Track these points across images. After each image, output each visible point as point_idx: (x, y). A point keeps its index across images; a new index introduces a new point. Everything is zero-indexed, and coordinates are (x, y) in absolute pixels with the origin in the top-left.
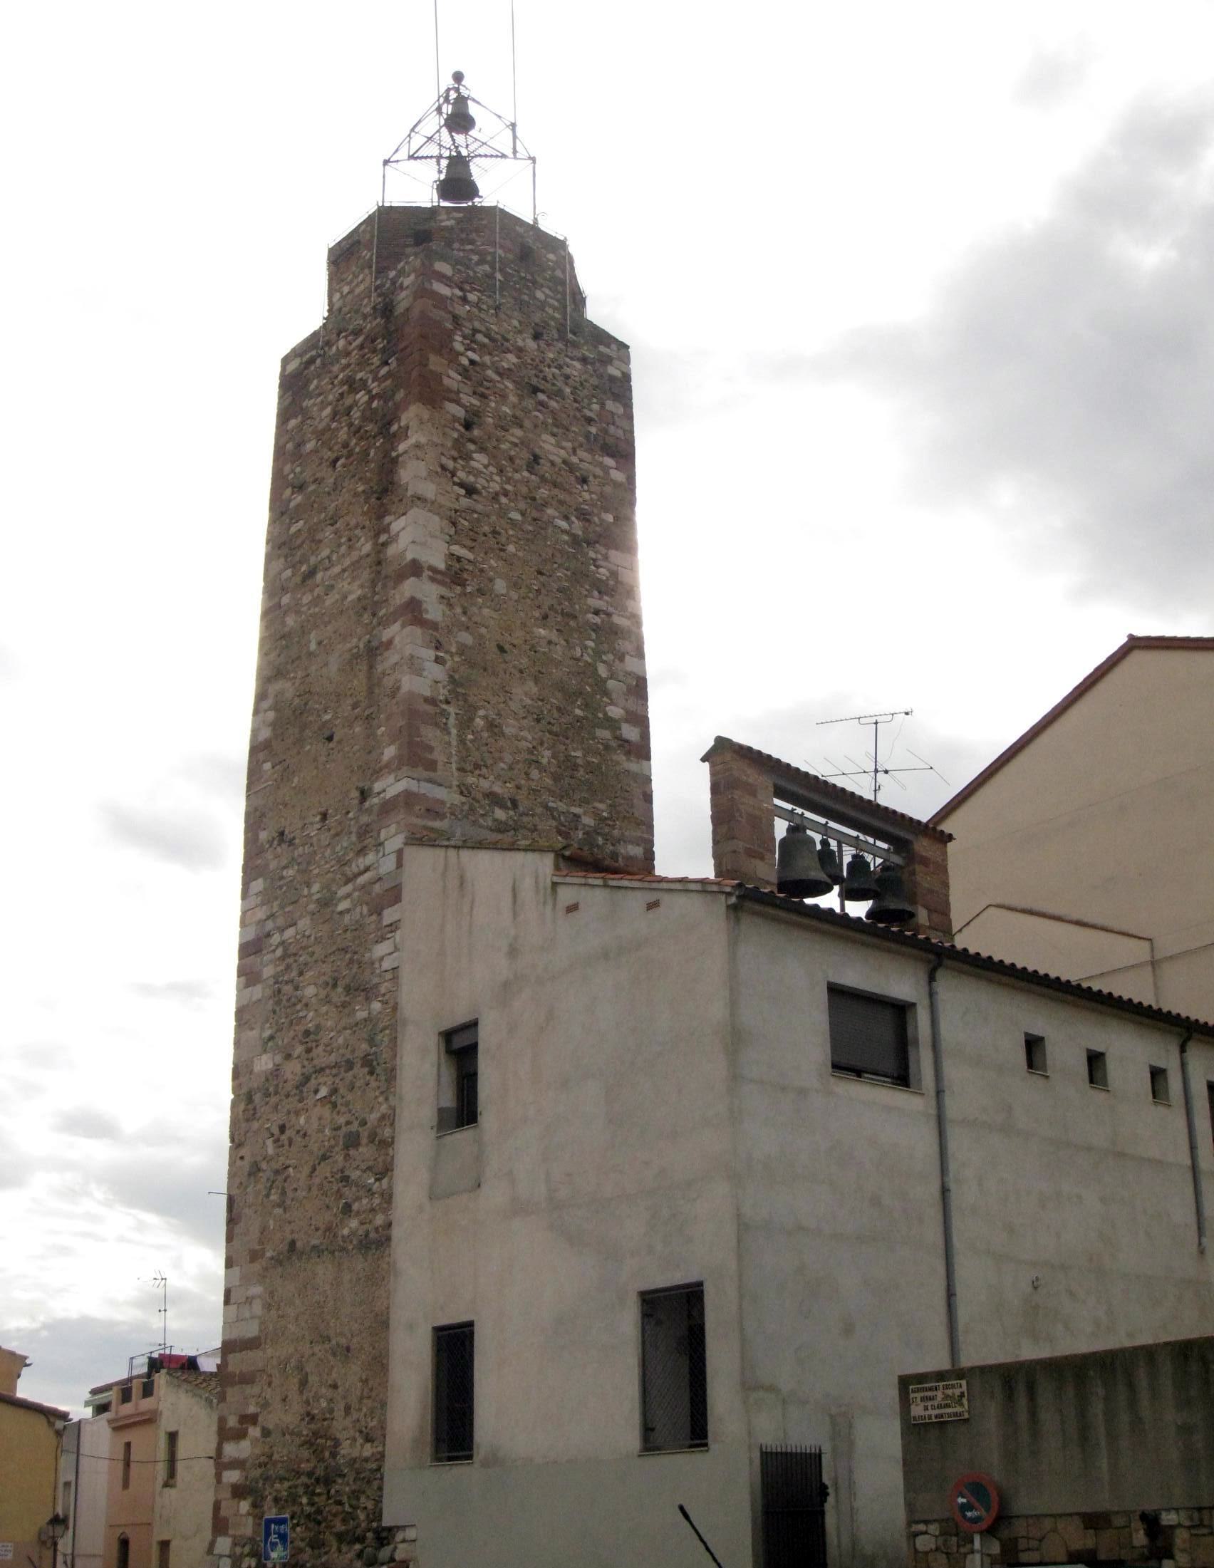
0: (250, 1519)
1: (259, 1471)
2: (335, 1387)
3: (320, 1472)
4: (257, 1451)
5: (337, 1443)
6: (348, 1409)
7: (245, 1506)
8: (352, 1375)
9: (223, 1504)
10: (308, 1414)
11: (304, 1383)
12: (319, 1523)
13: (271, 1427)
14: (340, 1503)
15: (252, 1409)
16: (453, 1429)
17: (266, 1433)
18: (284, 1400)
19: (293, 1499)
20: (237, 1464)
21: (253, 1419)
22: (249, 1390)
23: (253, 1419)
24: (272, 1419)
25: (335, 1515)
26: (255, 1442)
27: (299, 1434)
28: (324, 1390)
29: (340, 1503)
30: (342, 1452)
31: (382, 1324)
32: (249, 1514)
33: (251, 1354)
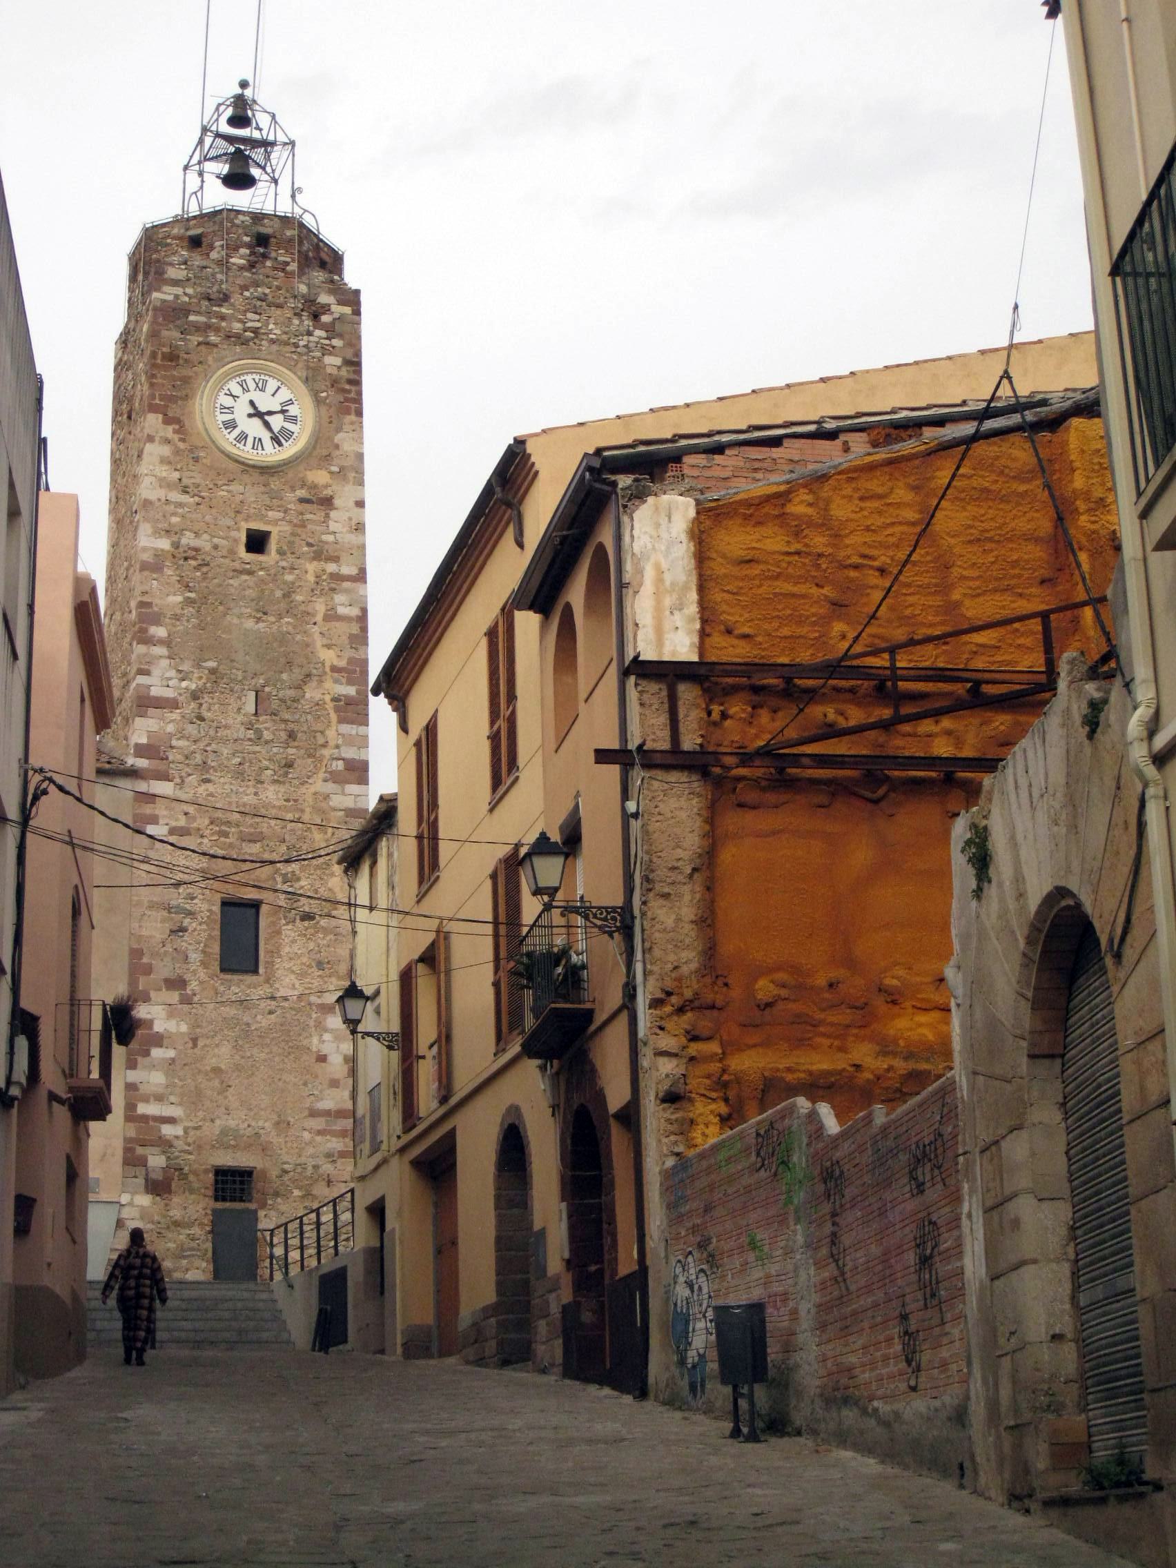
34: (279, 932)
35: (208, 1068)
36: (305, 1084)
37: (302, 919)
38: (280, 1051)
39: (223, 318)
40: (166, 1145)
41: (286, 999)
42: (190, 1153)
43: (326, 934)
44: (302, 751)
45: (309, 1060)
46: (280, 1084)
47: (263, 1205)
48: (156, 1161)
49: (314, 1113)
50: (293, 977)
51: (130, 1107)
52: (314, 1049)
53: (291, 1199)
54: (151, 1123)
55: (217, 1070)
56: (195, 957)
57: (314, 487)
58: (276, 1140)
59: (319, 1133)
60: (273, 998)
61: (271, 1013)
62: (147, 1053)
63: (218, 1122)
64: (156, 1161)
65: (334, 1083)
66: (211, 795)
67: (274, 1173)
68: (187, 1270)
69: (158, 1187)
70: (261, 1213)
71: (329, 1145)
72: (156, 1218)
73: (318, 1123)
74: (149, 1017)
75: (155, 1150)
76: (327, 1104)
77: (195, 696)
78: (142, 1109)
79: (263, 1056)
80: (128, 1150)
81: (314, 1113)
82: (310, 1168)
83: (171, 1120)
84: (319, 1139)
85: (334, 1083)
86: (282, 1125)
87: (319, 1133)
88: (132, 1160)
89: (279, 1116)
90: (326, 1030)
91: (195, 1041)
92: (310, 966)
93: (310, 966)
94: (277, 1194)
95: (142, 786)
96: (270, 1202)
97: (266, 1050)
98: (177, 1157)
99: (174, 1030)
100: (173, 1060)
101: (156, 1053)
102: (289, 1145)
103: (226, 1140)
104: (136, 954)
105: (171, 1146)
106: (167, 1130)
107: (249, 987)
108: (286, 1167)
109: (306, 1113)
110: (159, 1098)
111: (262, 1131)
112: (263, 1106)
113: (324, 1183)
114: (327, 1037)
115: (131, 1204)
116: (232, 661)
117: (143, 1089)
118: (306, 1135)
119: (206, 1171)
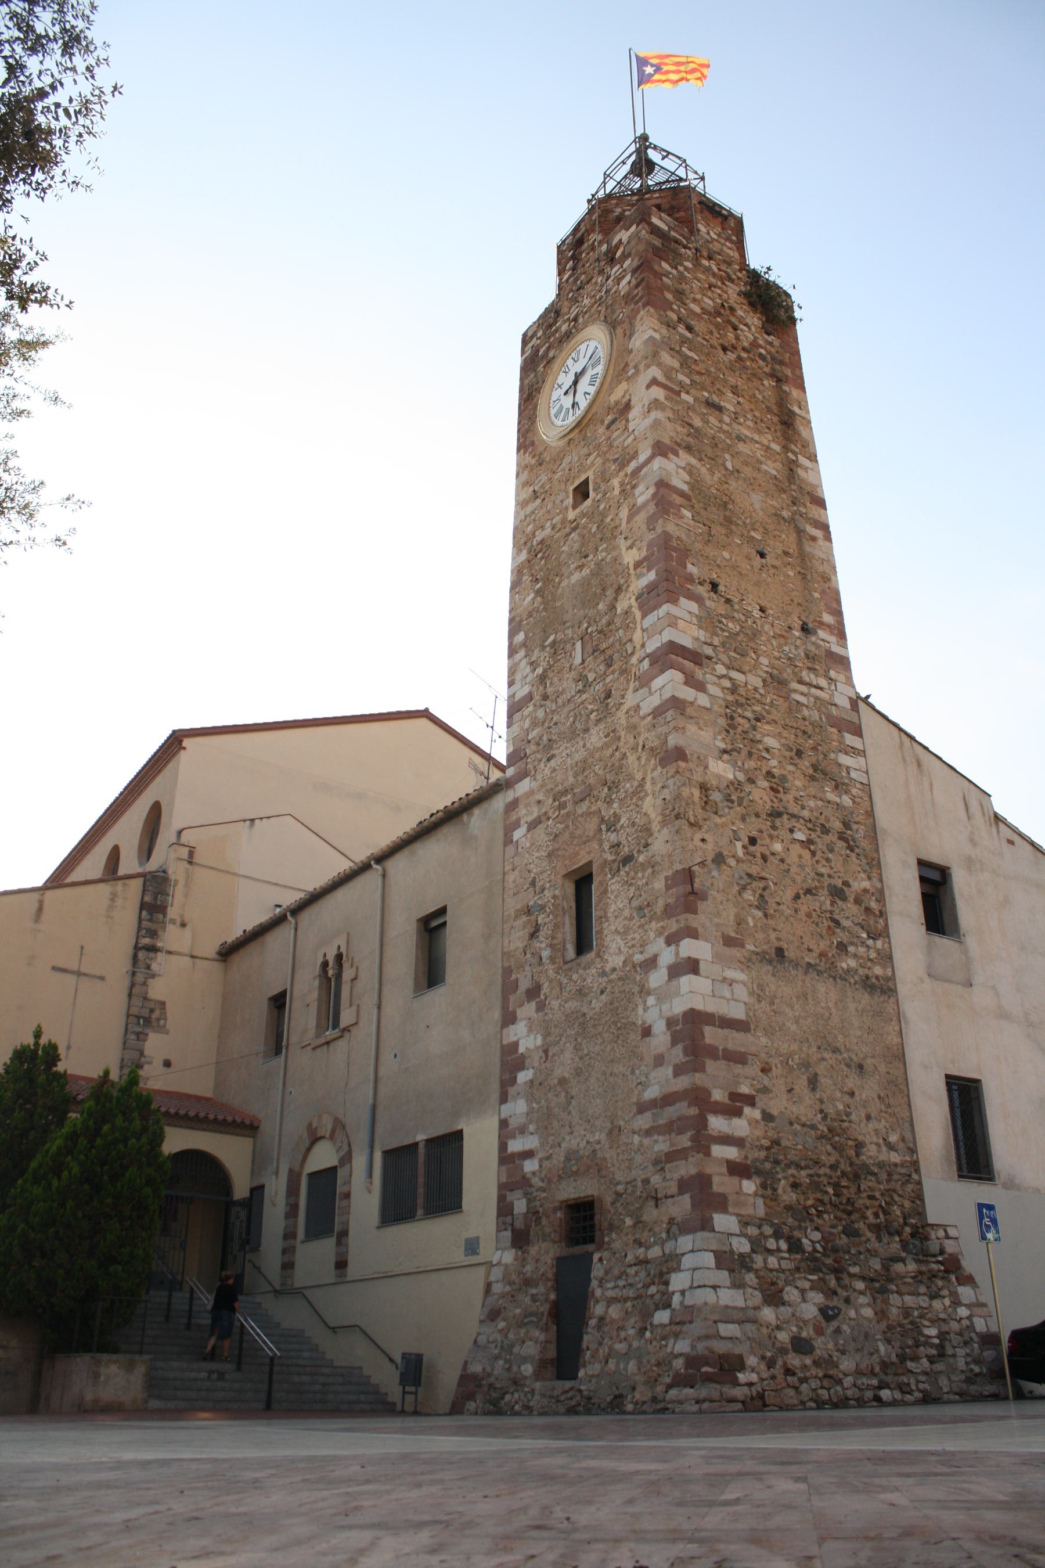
0: (760, 1202)
1: (763, 1154)
2: (852, 1094)
3: (844, 1166)
4: (758, 1133)
5: (859, 1146)
6: (868, 1117)
7: (749, 1186)
8: (869, 1090)
9: (716, 1180)
10: (821, 1111)
11: (813, 1083)
12: (849, 1213)
13: (775, 1113)
14: (871, 1197)
15: (745, 1089)
16: (973, 1156)
17: (767, 1117)
18: (790, 1091)
19: (815, 1186)
20: (727, 1140)
21: (751, 1101)
22: (738, 1069)
23: (751, 1101)
24: (778, 1105)
25: (867, 1208)
26: (753, 1123)
27: (813, 1127)
28: (838, 1094)
29: (871, 1197)
30: (869, 1154)
31: (899, 1056)
32: (756, 1194)
33: (735, 1034)
34: (606, 891)
35: (556, 1081)
36: (633, 1072)
37: (624, 866)
38: (611, 1036)
39: (556, 331)
40: (522, 1183)
41: (614, 970)
42: (544, 1191)
43: (644, 871)
44: (617, 673)
45: (634, 1037)
46: (611, 1079)
47: (600, 1247)
48: (520, 1206)
49: (642, 1108)
50: (618, 938)
51: (503, 1146)
52: (640, 1022)
53: (625, 1231)
54: (517, 1162)
55: (563, 1081)
56: (546, 954)
57: (617, 403)
58: (610, 1154)
59: (648, 1133)
60: (604, 974)
61: (602, 992)
62: (513, 1081)
63: (563, 1145)
64: (520, 1206)
65: (659, 1061)
66: (554, 770)
67: (608, 1199)
68: (523, 1342)
69: (520, 1240)
70: (596, 1257)
71: (656, 1148)
72: (514, 1277)
73: (644, 1121)
74: (515, 1039)
75: (519, 1193)
76: (652, 1092)
77: (542, 679)
78: (515, 1146)
79: (597, 1048)
80: (501, 1198)
81: (642, 1108)
82: (640, 1184)
83: (528, 1154)
84: (646, 1141)
85: (659, 1061)
86: (614, 1132)
87: (648, 1133)
88: (504, 1209)
89: (612, 1123)
90: (649, 993)
91: (546, 1052)
92: (631, 918)
93: (631, 918)
94: (611, 1227)
95: (510, 795)
96: (606, 1239)
97: (600, 1040)
98: (535, 1198)
99: (532, 1047)
100: (532, 1081)
101: (523, 1077)
102: (621, 1157)
103: (579, 1164)
104: (507, 972)
105: (531, 1186)
106: (530, 1166)
107: (585, 969)
108: (620, 1188)
109: (634, 1109)
110: (522, 1130)
111: (598, 1147)
112: (597, 1115)
113: (652, 1203)
114: (651, 1000)
115: (499, 1263)
116: (564, 623)
117: (513, 1123)
118: (636, 1139)
119: (555, 1210)
